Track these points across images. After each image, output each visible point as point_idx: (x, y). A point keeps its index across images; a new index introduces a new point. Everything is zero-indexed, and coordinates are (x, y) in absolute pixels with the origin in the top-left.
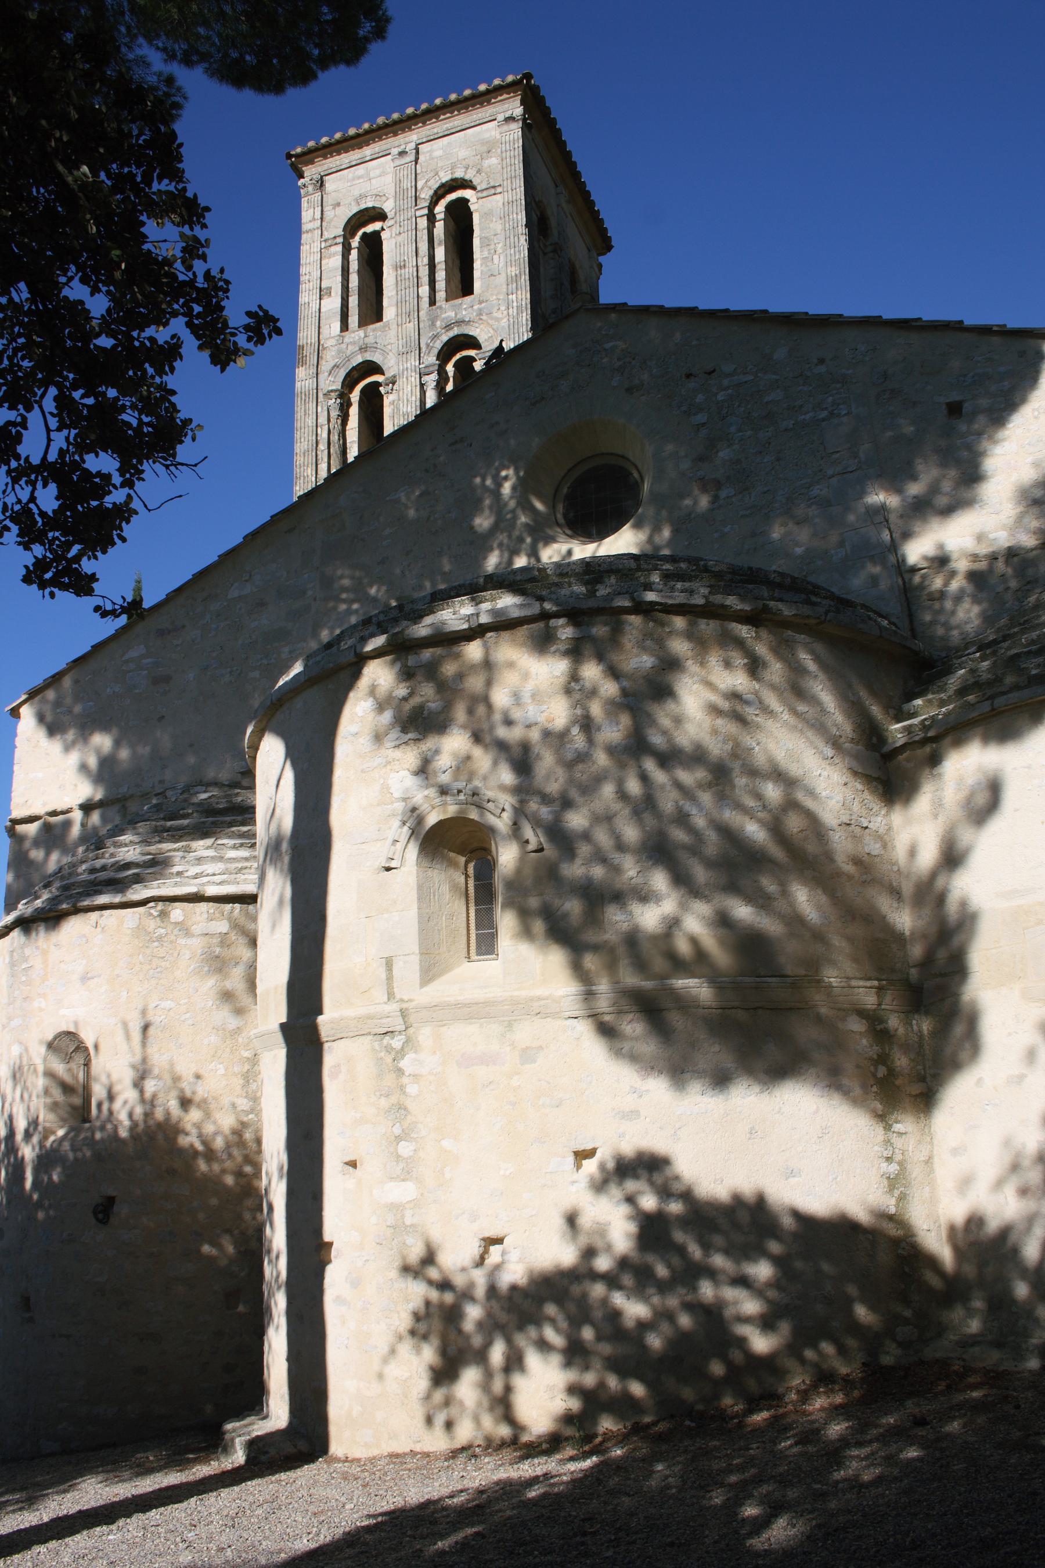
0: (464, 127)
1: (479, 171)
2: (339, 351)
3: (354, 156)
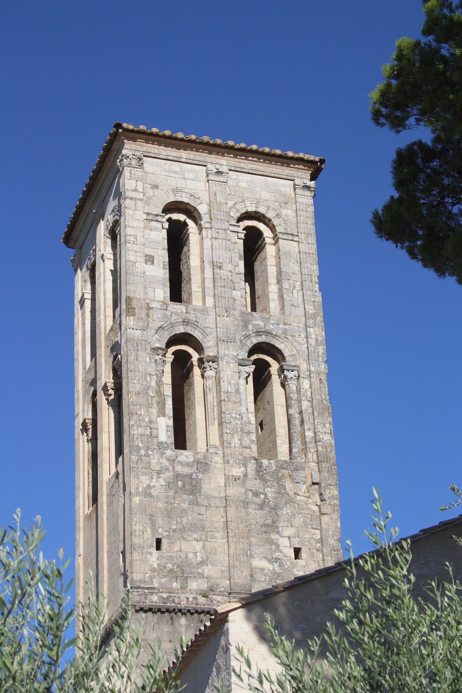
0: (265, 174)
1: (278, 215)
2: (165, 316)
3: (172, 152)
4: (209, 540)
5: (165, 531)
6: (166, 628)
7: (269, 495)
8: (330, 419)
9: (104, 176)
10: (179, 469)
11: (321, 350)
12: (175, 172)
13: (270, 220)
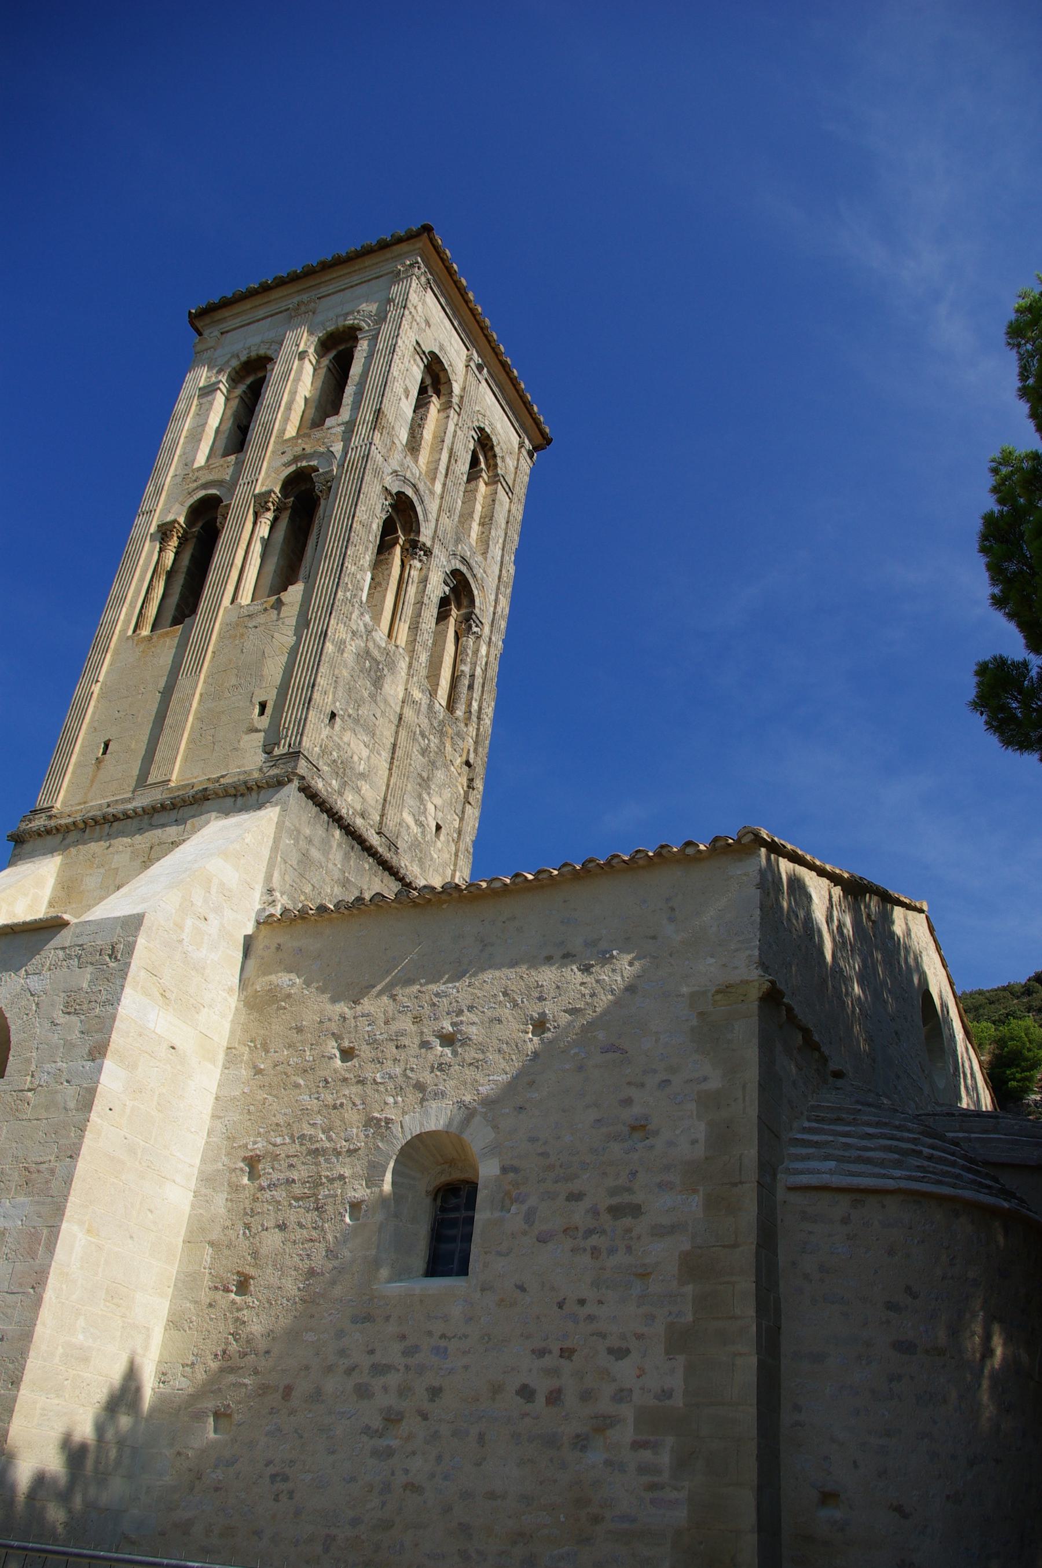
4: (375, 753)
5: (341, 709)
6: (320, 832)
7: (432, 745)
8: (493, 704)
9: (345, 271)
10: (371, 645)
11: (503, 624)
12: (446, 328)
13: (495, 456)
